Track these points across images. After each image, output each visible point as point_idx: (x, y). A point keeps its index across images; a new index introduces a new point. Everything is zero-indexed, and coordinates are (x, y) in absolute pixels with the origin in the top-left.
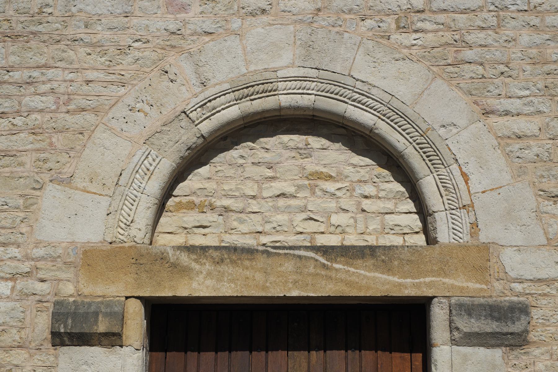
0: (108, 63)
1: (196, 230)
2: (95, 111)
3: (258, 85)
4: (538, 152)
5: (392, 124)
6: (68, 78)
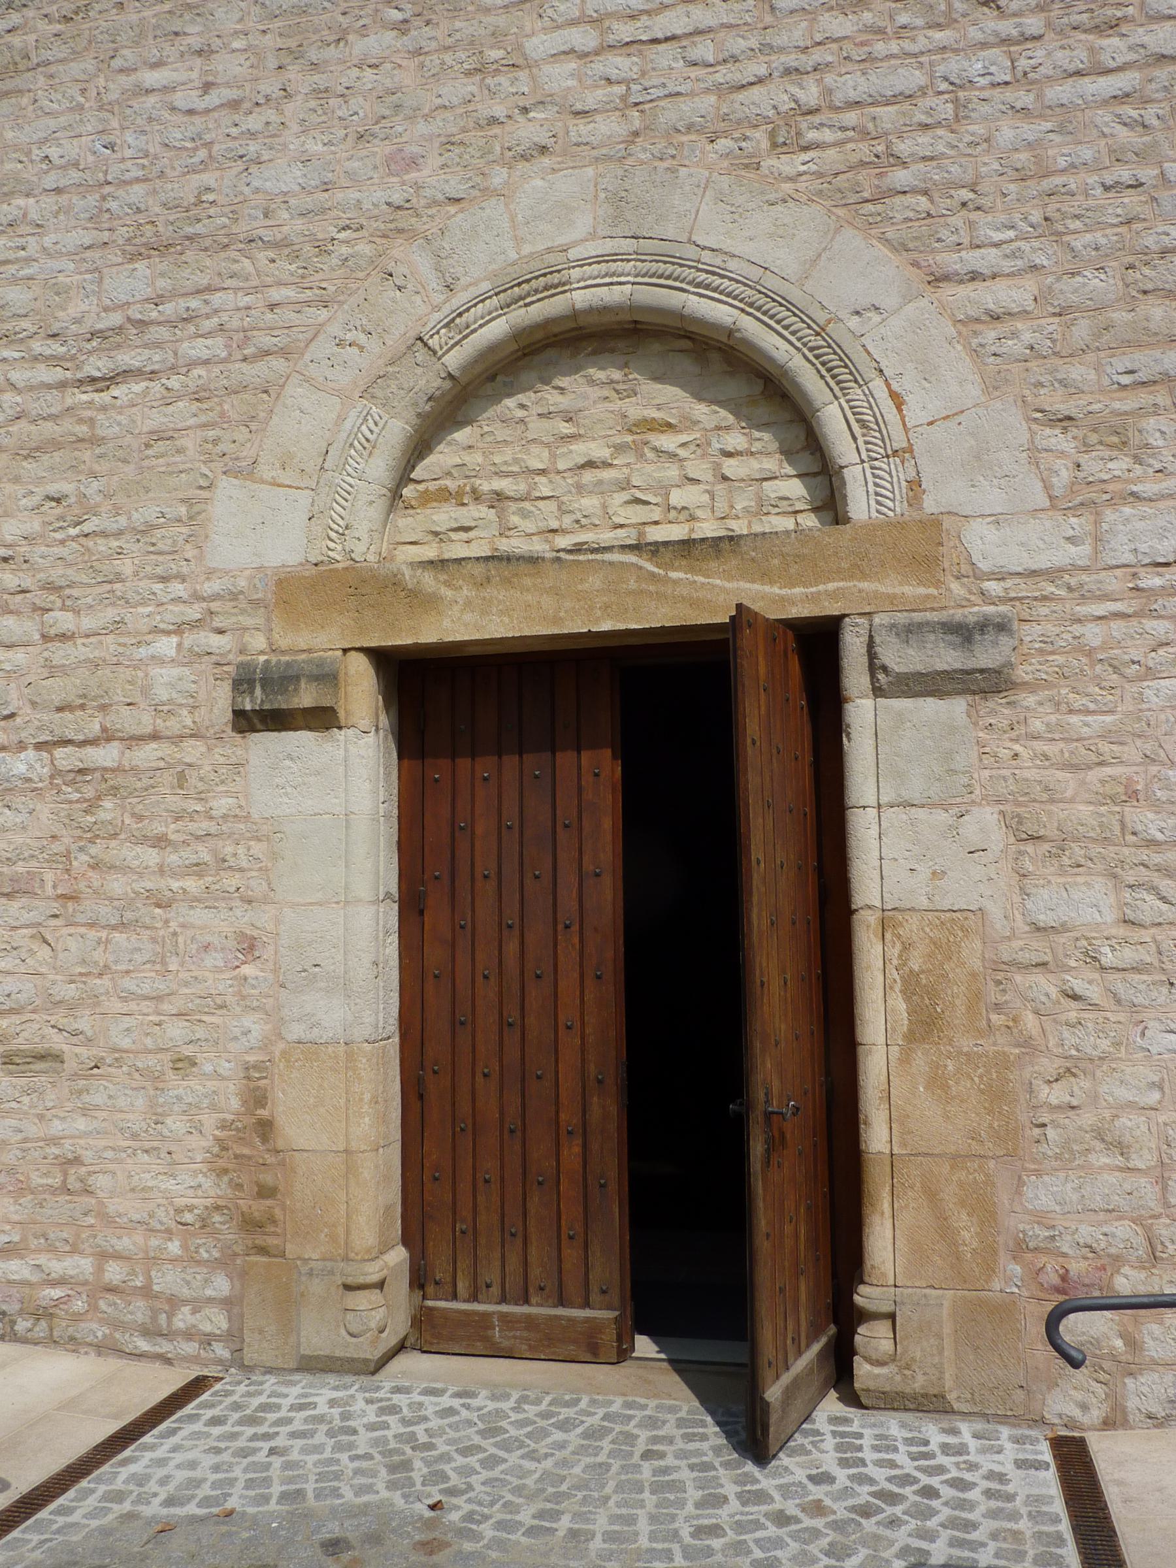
0: (300, 271)
1: (453, 535)
2: (284, 352)
3: (537, 278)
4: (1032, 341)
5: (765, 319)
6: (241, 305)
